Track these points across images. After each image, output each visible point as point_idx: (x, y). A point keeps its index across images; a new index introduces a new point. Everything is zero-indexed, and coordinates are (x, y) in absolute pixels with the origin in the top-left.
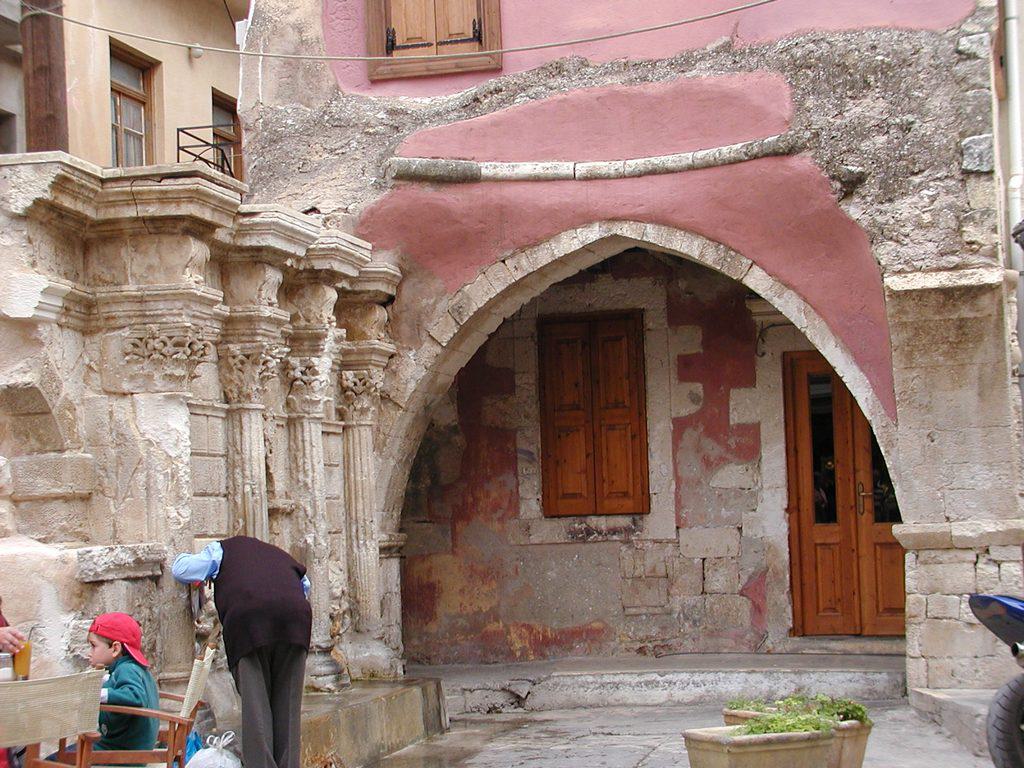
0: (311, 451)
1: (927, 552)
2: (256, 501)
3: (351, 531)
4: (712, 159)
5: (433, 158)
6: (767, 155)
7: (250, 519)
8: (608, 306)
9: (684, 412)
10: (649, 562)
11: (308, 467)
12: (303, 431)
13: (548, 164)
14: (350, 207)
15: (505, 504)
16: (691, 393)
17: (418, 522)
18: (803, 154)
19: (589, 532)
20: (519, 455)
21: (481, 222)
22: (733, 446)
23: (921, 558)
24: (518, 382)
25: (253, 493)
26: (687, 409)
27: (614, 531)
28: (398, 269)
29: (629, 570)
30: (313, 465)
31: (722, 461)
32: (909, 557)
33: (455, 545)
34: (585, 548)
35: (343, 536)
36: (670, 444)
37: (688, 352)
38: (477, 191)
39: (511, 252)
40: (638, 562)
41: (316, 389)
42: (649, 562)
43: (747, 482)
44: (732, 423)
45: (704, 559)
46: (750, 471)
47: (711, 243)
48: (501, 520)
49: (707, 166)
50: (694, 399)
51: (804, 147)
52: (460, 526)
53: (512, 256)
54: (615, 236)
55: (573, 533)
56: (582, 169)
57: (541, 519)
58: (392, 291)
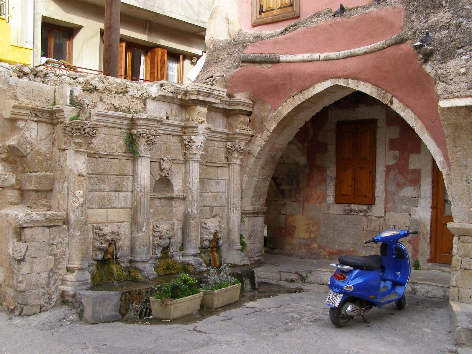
0: (192, 174)
1: (464, 237)
2: (142, 195)
3: (228, 206)
4: (373, 48)
5: (260, 54)
6: (393, 45)
7: (139, 202)
8: (364, 117)
9: (390, 164)
10: (373, 225)
11: (191, 180)
12: (189, 166)
13: (309, 55)
14: (225, 75)
15: (321, 197)
16: (394, 155)
17: (292, 201)
18: (407, 42)
19: (351, 211)
20: (328, 178)
21: (282, 80)
22: (410, 179)
23: (461, 240)
24: (329, 148)
25: (141, 192)
26: (391, 162)
27: (360, 211)
28: (251, 101)
29: (365, 228)
30: (193, 180)
31: (405, 185)
32: (455, 238)
33: (303, 212)
34: (349, 217)
35: (226, 208)
36: (384, 177)
37: (393, 138)
38: (279, 67)
39: (296, 93)
40: (369, 225)
41: (194, 149)
42: (373, 225)
43: (414, 194)
44: (409, 169)
45: (395, 226)
46: (416, 190)
47: (375, 87)
48: (319, 203)
49: (372, 52)
50: (395, 158)
51: (408, 39)
52: (305, 204)
53: (297, 94)
54: (337, 86)
55: (345, 211)
56: (323, 56)
57: (334, 204)
58: (251, 110)
